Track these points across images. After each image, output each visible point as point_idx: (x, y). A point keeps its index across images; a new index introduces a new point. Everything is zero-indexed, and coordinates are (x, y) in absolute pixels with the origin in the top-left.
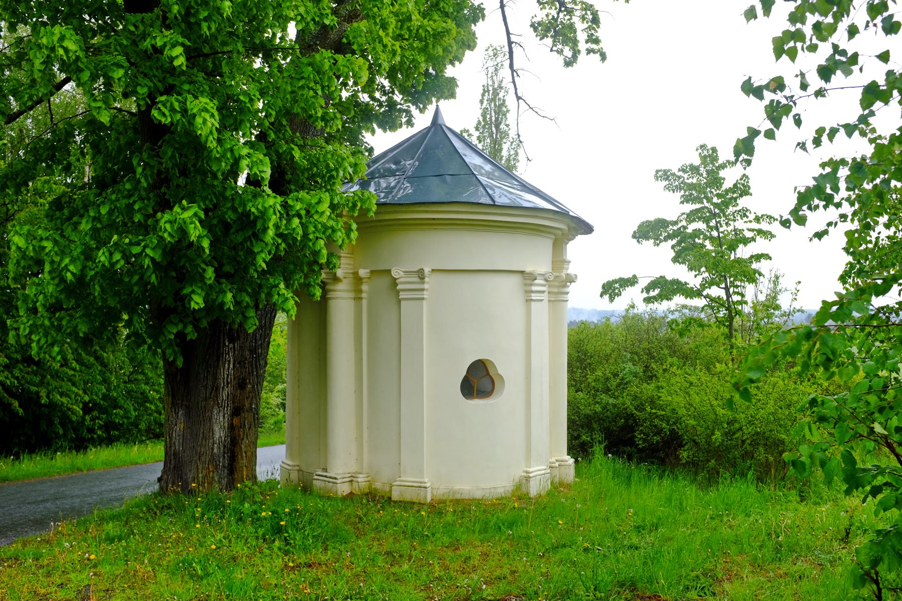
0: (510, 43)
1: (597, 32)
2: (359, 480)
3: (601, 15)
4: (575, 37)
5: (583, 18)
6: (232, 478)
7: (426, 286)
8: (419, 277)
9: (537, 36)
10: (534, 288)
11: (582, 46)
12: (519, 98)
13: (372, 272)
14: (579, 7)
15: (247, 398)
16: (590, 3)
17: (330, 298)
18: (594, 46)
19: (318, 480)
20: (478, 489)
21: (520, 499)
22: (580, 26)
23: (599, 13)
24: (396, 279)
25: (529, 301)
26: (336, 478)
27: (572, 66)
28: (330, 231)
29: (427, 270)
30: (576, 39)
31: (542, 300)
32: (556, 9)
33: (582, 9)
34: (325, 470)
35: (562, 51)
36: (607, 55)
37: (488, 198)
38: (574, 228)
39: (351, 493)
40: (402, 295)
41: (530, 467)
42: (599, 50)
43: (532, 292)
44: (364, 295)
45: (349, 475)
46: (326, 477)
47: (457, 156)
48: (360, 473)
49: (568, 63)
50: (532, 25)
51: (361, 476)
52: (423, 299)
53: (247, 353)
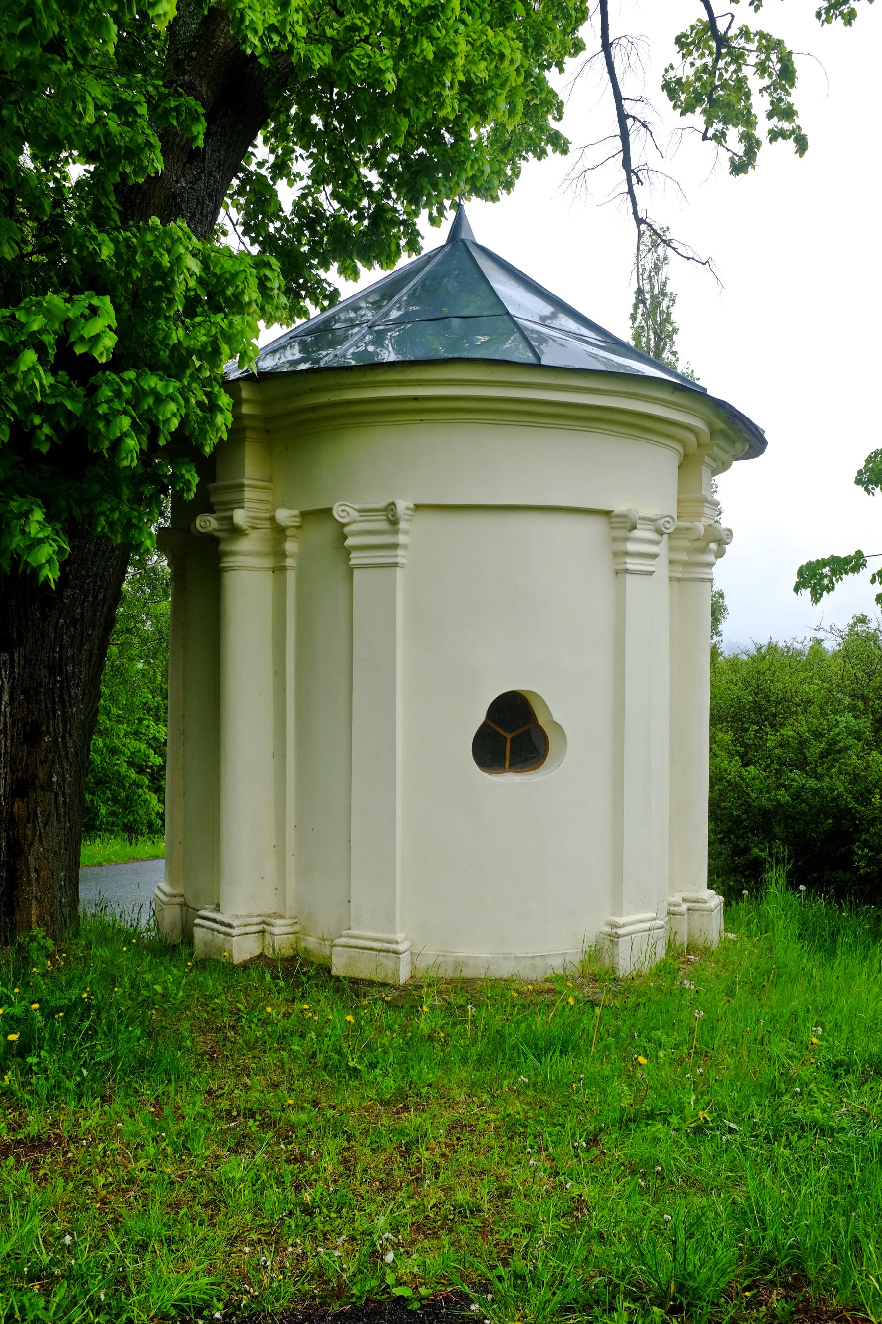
0: (623, 117)
1: (789, 94)
2: (276, 930)
3: (798, 62)
4: (748, 108)
5: (762, 68)
6: (12, 921)
7: (402, 539)
8: (388, 520)
9: (675, 107)
10: (631, 547)
11: (762, 128)
12: (640, 221)
13: (304, 515)
14: (752, 46)
15: (42, 763)
16: (776, 36)
17: (226, 570)
18: (786, 125)
19: (202, 926)
20: (506, 959)
21: (595, 979)
22: (755, 83)
23: (794, 57)
24: (344, 525)
25: (621, 572)
26: (230, 926)
27: (746, 172)
28: (151, 401)
29: (402, 505)
30: (749, 112)
31: (651, 573)
32: (711, 54)
33: (759, 49)
34: (217, 909)
35: (723, 135)
36: (810, 142)
37: (522, 346)
38: (722, 432)
39: (262, 956)
40: (356, 558)
41: (621, 915)
42: (793, 132)
43: (627, 554)
44: (289, 562)
45: (259, 920)
46: (215, 921)
47: (484, 286)
48: (281, 917)
49: (739, 167)
50: (666, 86)
51: (279, 922)
52: (395, 565)
53: (43, 672)
